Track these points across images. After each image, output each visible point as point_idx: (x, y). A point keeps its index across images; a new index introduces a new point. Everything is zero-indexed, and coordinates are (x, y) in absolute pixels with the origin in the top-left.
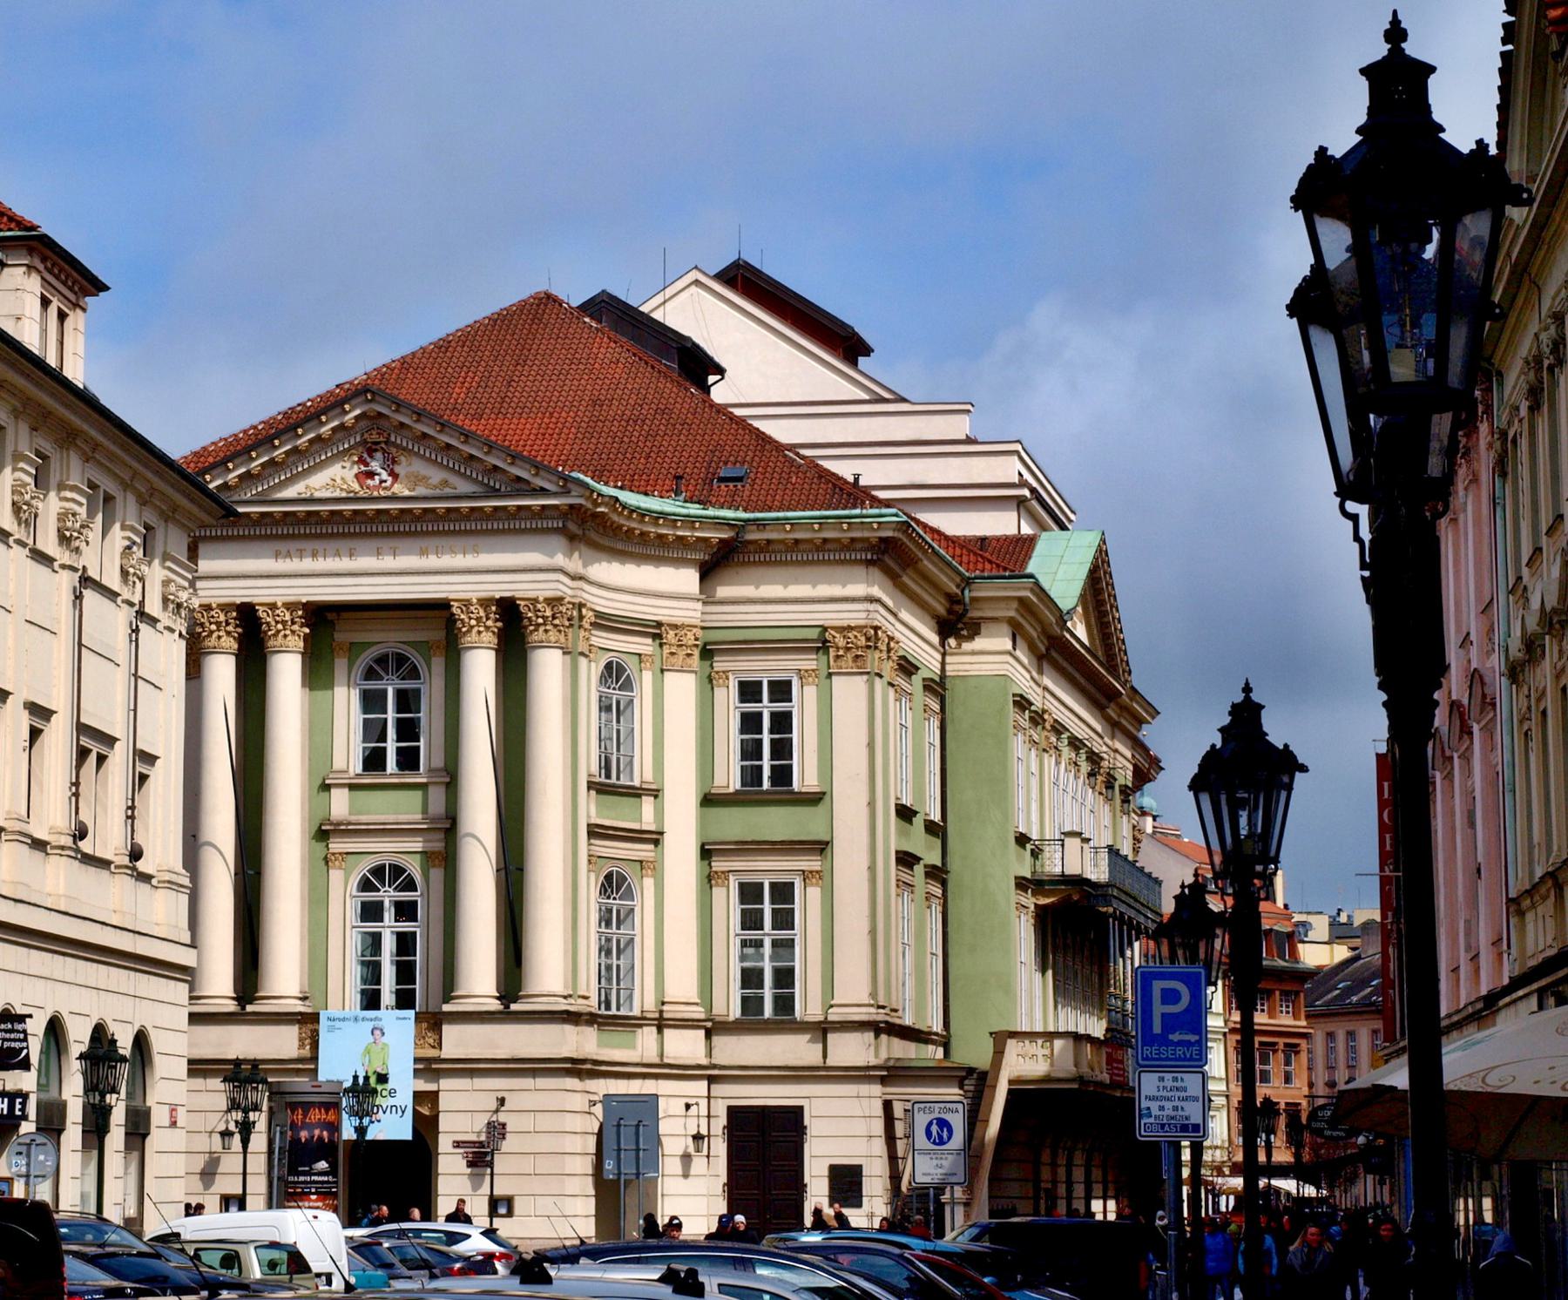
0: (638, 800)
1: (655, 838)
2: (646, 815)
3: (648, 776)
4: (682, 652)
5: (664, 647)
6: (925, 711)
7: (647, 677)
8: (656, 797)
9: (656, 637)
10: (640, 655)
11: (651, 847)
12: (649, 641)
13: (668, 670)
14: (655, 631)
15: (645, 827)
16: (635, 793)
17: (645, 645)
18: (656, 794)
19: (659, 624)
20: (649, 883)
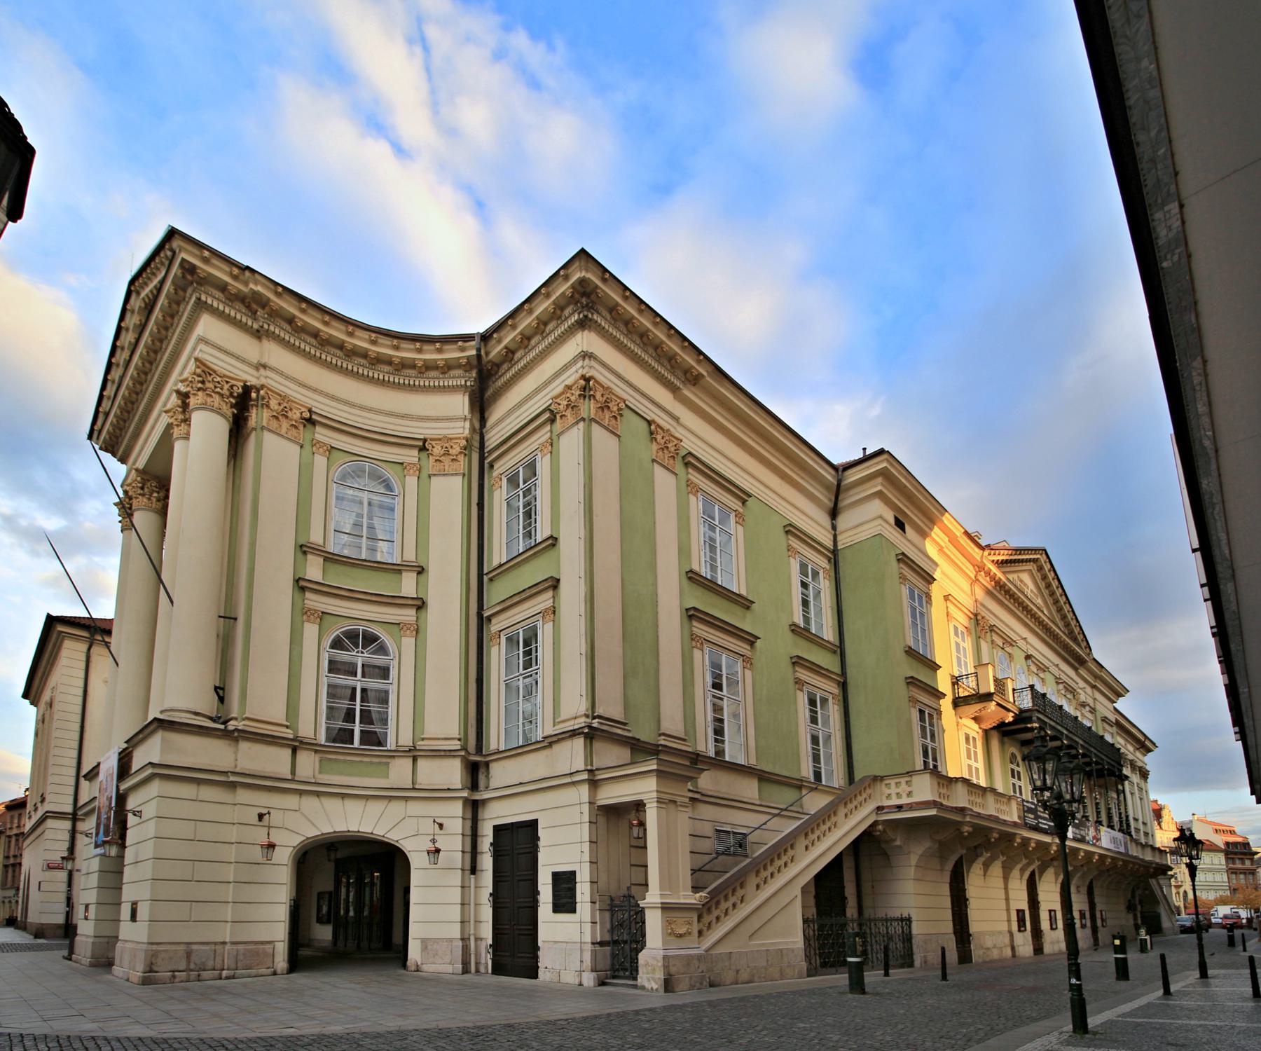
0: (398, 576)
1: (420, 605)
2: (408, 585)
3: (410, 556)
4: (446, 460)
5: (431, 457)
6: (789, 550)
7: (411, 481)
8: (419, 573)
9: (423, 449)
10: (402, 464)
11: (413, 612)
12: (415, 452)
13: (434, 475)
14: (423, 447)
15: (401, 595)
16: (396, 569)
17: (411, 456)
18: (421, 571)
19: (425, 440)
20: (408, 642)
